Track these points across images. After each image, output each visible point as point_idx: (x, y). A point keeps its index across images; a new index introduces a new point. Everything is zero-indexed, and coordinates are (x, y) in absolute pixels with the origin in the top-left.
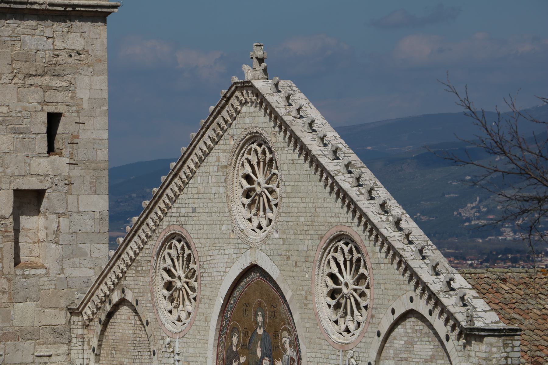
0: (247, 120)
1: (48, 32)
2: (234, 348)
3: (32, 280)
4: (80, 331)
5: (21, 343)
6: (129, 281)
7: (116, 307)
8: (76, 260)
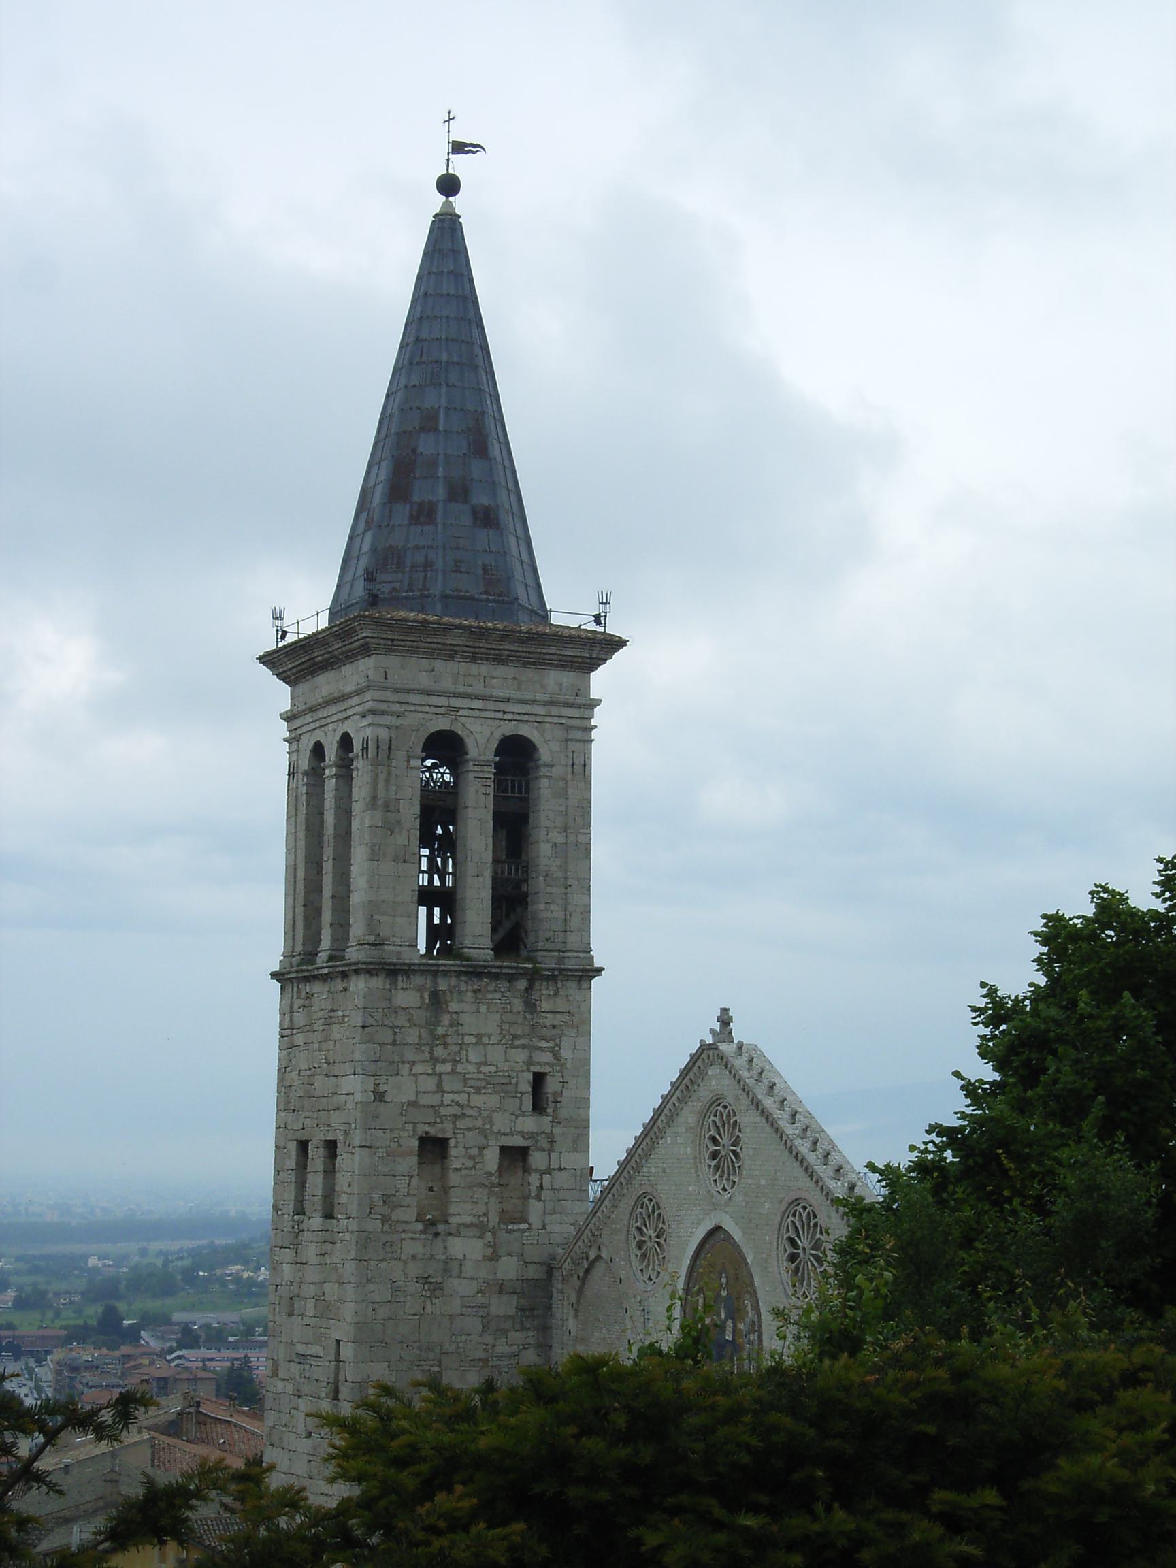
7: (592, 1264)
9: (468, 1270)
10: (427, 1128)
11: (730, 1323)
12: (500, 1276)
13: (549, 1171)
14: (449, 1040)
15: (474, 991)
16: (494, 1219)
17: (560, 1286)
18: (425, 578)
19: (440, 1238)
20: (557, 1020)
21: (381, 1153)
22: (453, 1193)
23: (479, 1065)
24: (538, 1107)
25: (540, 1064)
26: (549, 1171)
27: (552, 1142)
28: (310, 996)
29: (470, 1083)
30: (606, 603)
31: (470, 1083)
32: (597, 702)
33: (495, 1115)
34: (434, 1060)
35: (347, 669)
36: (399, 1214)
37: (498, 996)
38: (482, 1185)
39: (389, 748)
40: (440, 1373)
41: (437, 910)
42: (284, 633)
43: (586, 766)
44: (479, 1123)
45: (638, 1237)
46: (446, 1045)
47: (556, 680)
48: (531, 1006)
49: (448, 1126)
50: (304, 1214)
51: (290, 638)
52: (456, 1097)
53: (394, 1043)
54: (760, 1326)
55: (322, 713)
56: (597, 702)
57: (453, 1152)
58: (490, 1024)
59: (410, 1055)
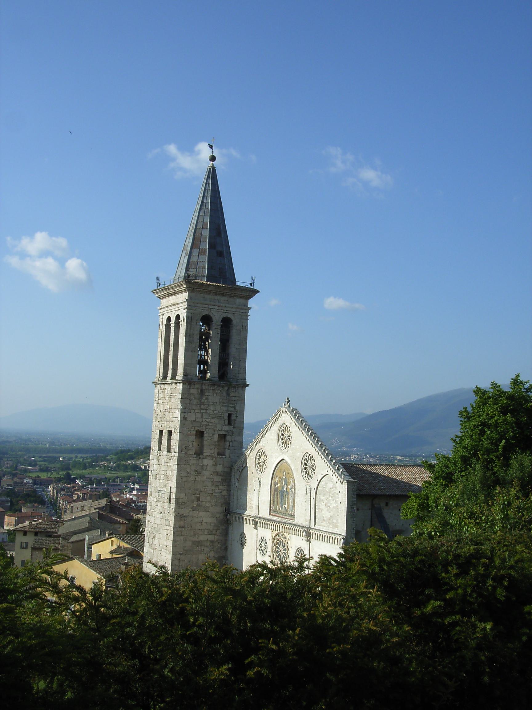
4: (234, 474)
9: (208, 468)
10: (198, 428)
11: (285, 486)
12: (217, 470)
13: (232, 441)
14: (205, 403)
15: (213, 390)
16: (216, 454)
17: (234, 474)
18: (203, 270)
19: (201, 459)
20: (236, 398)
22: (205, 447)
23: (213, 411)
24: (229, 423)
25: (231, 411)
26: (232, 441)
27: (233, 433)
28: (164, 389)
29: (211, 416)
30: (254, 280)
31: (211, 416)
32: (251, 308)
33: (217, 425)
34: (201, 409)
35: (179, 296)
36: (189, 452)
37: (219, 391)
38: (213, 445)
39: (191, 319)
40: (200, 497)
41: (202, 366)
42: (160, 284)
43: (246, 326)
44: (213, 427)
46: (204, 405)
47: (239, 301)
48: (228, 394)
49: (204, 427)
50: (161, 451)
51: (161, 286)
52: (207, 420)
53: (190, 404)
54: (295, 487)
55: (170, 308)
56: (251, 308)
57: (205, 435)
58: (217, 399)
59: (194, 407)
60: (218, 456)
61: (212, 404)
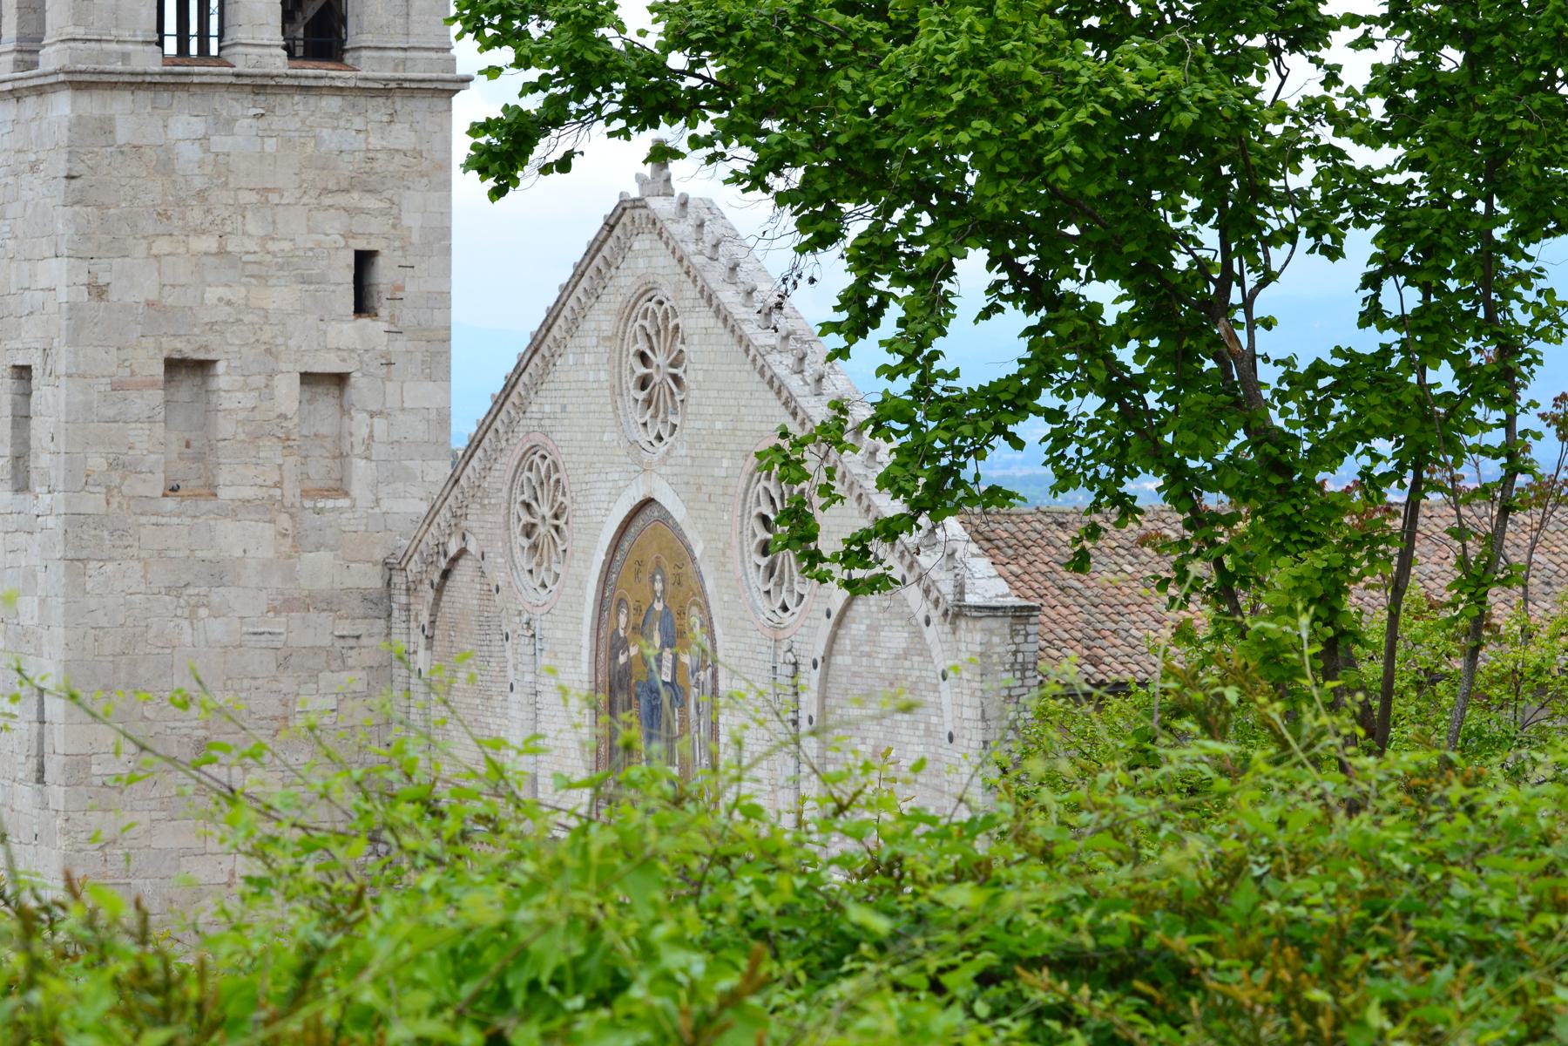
0: (641, 262)
1: (358, 122)
2: (622, 633)
3: (329, 517)
4: (403, 599)
5: (313, 615)
6: (472, 522)
8: (400, 486)
16: (291, 492)
17: (403, 599)
21: (103, 385)
24: (362, 305)
45: (526, 518)
60: (308, 503)
61: (253, 197)
